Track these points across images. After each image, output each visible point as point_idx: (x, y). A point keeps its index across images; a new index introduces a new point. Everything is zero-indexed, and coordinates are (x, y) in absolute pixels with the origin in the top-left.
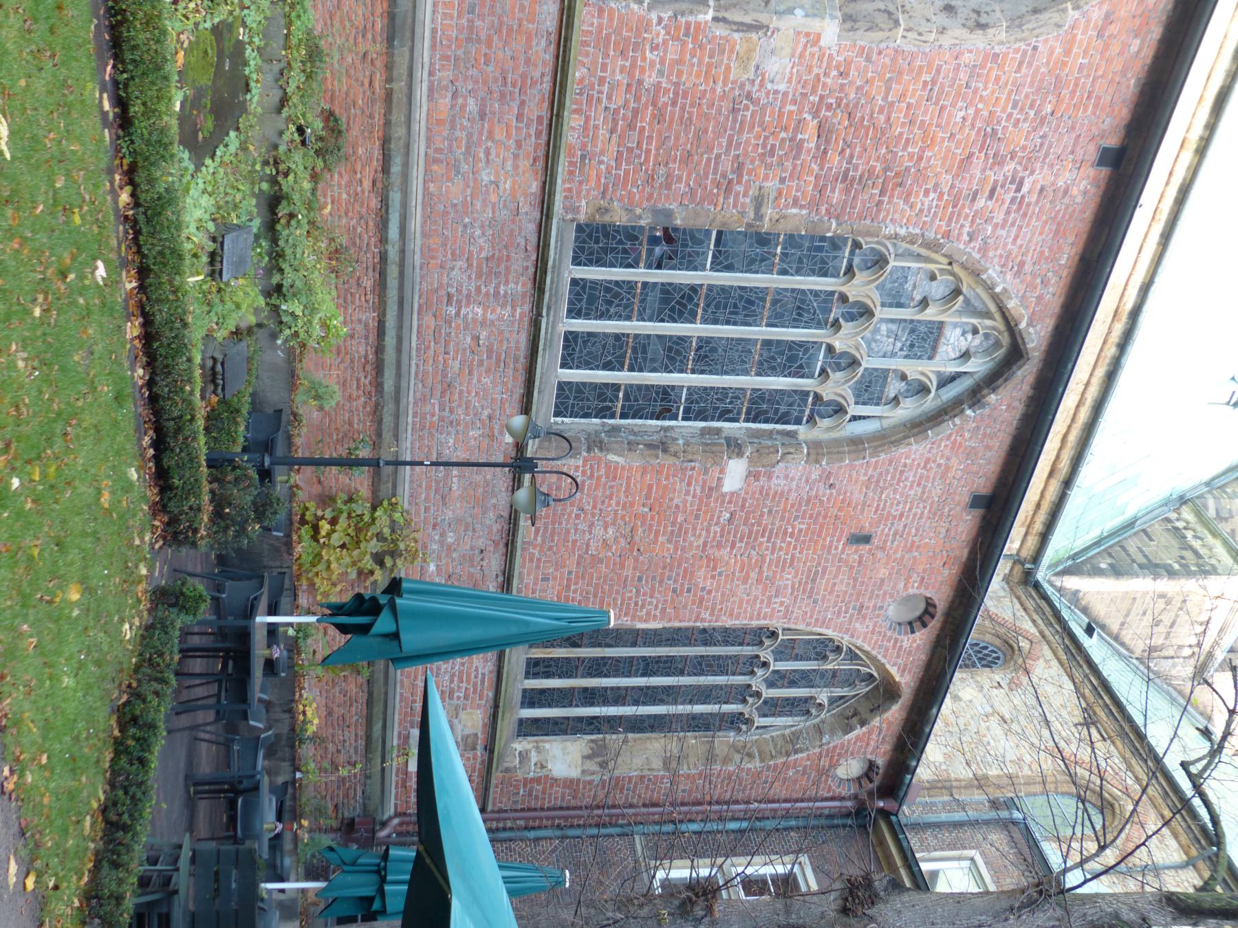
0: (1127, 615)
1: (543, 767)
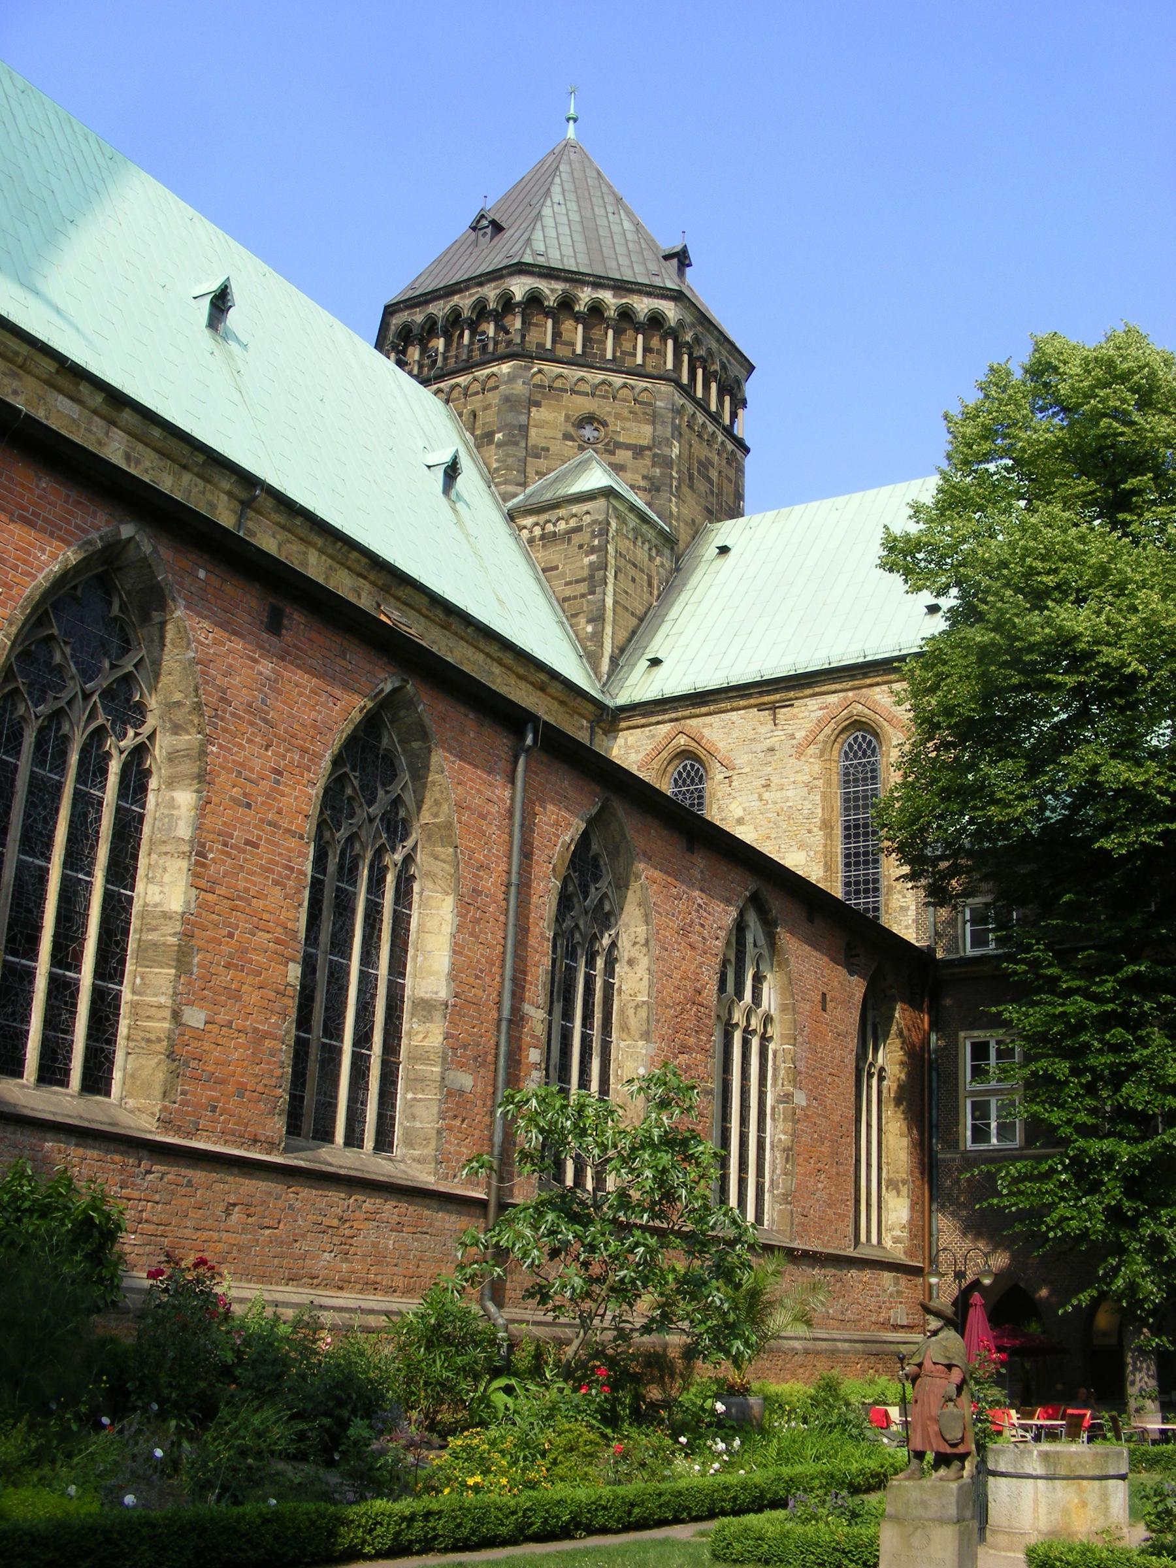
0: (626, 609)
1: (904, 1227)
